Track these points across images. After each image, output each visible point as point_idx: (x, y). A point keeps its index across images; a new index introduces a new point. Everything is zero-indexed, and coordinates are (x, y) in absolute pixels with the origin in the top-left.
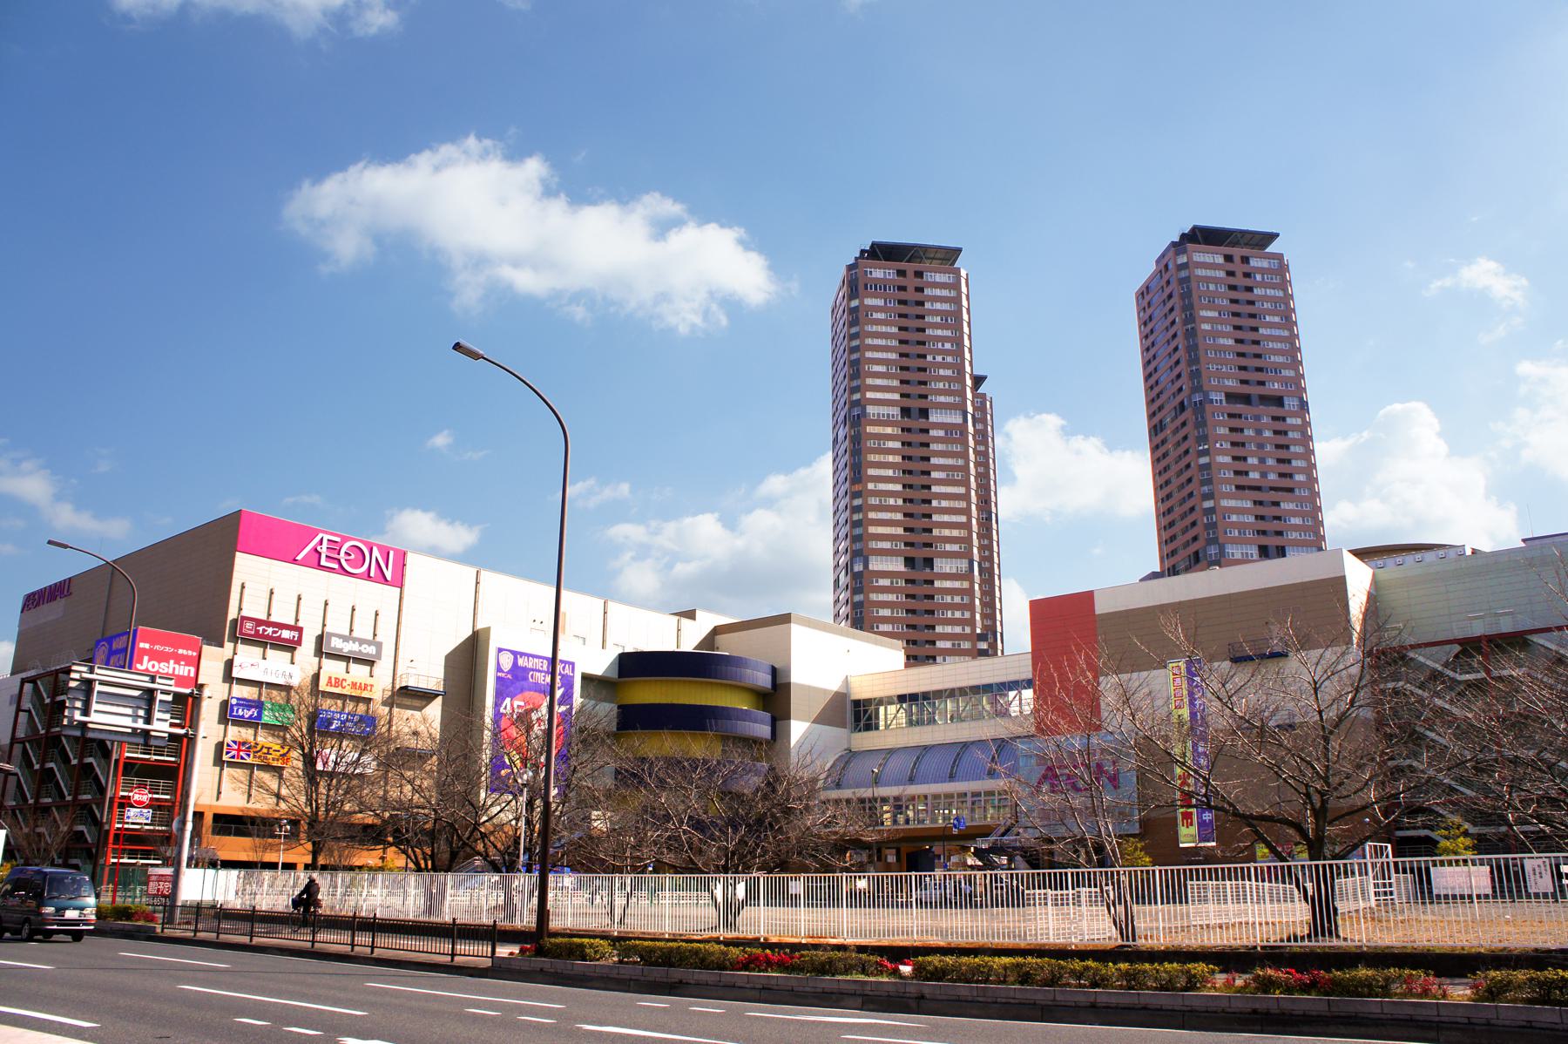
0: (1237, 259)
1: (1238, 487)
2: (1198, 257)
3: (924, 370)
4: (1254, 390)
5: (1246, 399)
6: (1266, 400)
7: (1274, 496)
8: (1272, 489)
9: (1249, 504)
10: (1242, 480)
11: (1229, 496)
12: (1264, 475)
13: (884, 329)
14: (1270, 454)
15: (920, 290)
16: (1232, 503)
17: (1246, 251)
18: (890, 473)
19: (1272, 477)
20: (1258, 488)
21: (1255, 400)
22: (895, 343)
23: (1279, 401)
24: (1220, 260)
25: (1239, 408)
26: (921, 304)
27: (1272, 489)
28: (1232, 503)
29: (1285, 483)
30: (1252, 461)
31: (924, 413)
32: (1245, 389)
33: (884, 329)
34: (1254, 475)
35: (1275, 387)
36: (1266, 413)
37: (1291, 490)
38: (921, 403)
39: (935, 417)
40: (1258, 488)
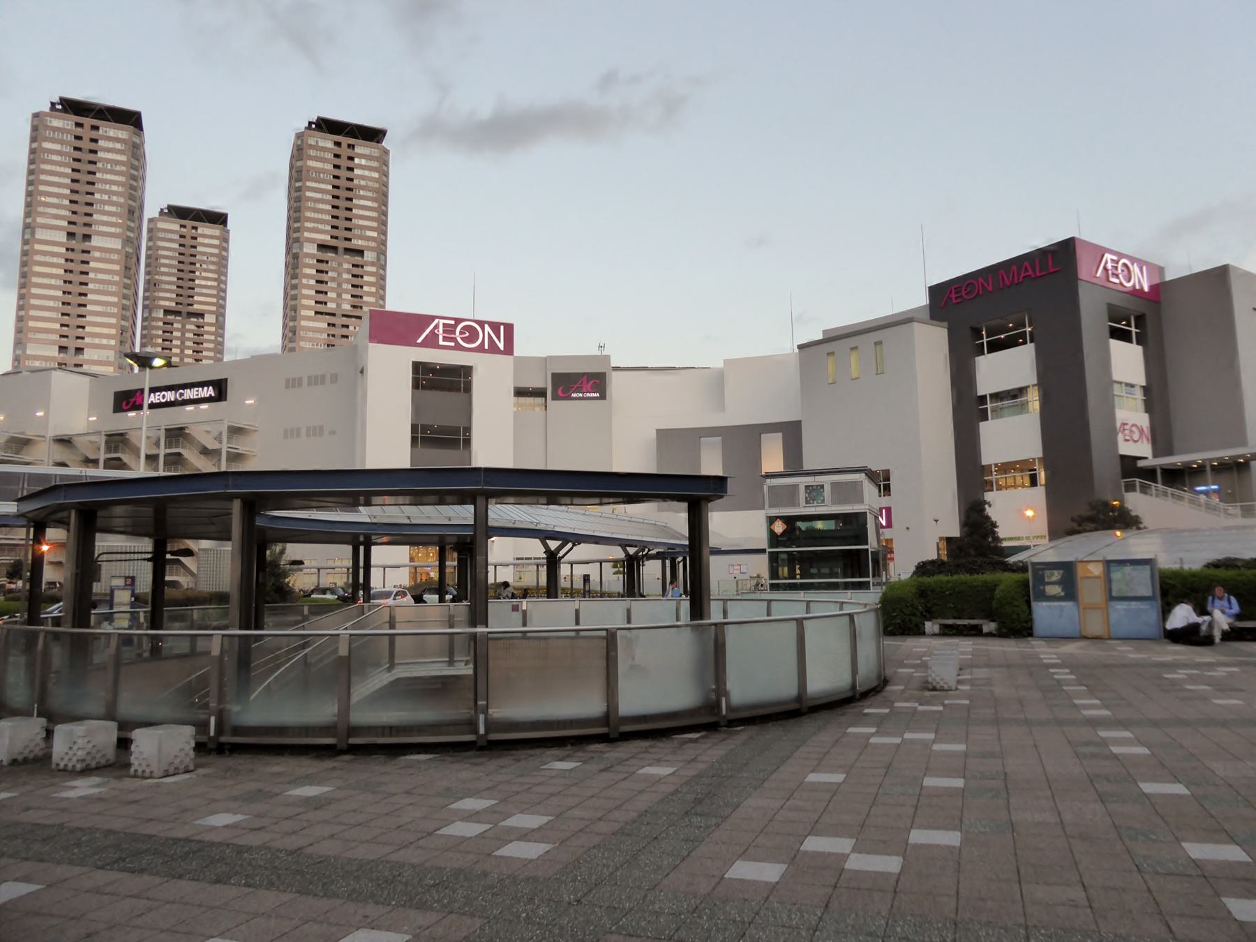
0: (344, 145)
1: (317, 313)
2: (312, 141)
3: (92, 205)
4: (342, 244)
5: (334, 249)
7: (345, 321)
8: (344, 316)
10: (321, 308)
11: (308, 318)
12: (339, 305)
13: (58, 169)
14: (346, 291)
15: (95, 141)
16: (311, 324)
17: (352, 141)
20: (334, 315)
21: (341, 251)
23: (360, 252)
24: (330, 145)
25: (329, 255)
26: (95, 152)
27: (344, 316)
28: (311, 324)
29: (357, 312)
30: (331, 295)
31: (87, 237)
32: (334, 243)
33: (58, 169)
34: (331, 306)
35: (357, 243)
36: (347, 263)
37: (360, 318)
38: (86, 231)
39: (96, 241)
40: (334, 315)
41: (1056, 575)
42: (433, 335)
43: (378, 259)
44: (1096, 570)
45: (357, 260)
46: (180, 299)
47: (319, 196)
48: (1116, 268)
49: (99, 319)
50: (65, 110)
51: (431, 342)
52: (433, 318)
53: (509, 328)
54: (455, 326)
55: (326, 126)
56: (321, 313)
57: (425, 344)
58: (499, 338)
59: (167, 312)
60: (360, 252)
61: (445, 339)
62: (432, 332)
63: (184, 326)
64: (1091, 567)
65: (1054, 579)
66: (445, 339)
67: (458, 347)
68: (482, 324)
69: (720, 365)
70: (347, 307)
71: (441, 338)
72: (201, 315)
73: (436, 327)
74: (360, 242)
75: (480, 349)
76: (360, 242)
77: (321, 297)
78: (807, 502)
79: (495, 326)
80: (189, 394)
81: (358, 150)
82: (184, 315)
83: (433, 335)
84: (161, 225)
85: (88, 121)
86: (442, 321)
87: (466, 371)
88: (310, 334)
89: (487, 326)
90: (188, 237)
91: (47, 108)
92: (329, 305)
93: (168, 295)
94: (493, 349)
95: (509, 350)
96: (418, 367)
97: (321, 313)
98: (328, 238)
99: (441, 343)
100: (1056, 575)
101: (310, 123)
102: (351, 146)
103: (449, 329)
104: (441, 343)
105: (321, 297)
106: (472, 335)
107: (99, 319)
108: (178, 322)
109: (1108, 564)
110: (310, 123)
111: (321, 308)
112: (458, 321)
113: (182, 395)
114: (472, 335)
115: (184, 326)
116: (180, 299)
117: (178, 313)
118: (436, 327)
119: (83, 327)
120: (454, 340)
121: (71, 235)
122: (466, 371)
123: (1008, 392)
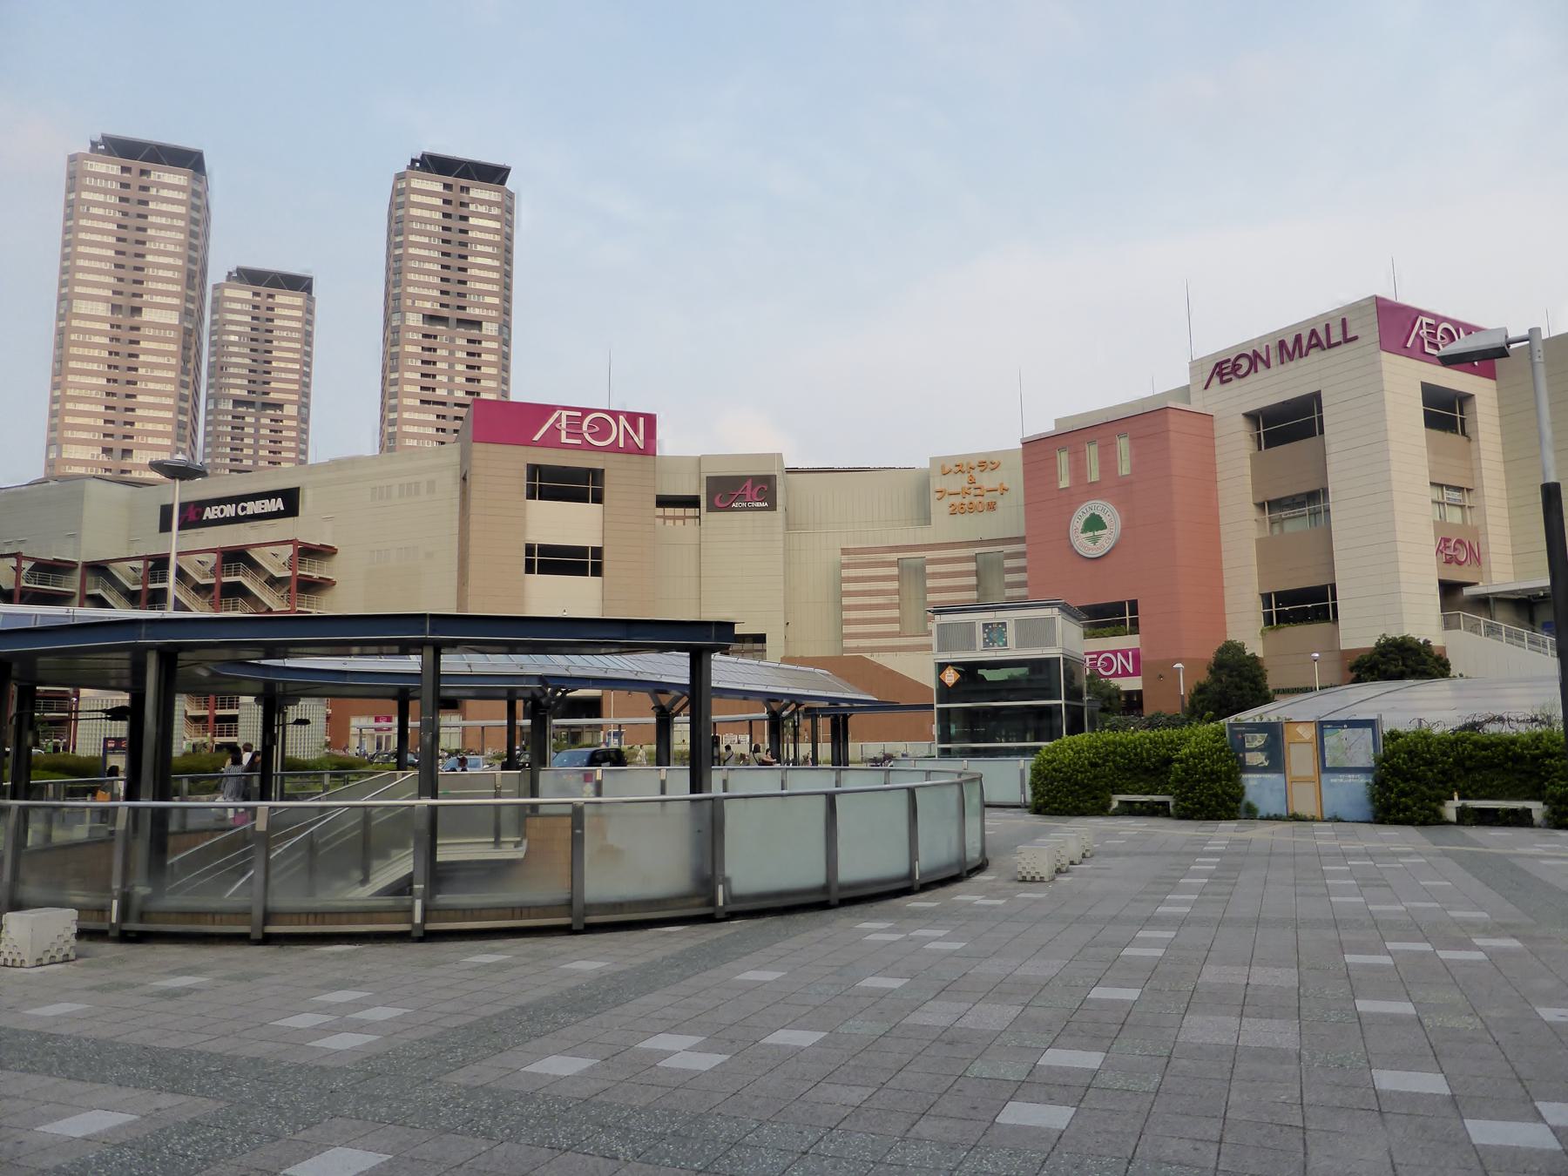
2: (416, 184)
6: (461, 322)
9: (433, 418)
10: (428, 395)
12: (451, 392)
16: (416, 416)
17: (464, 182)
18: (95, 367)
19: (460, 394)
20: (444, 404)
21: (453, 323)
22: (112, 240)
24: (439, 188)
28: (416, 416)
31: (137, 311)
32: (445, 312)
34: (441, 392)
35: (473, 312)
39: (148, 315)
40: (444, 404)
41: (1259, 740)
42: (554, 430)
43: (500, 331)
44: (1308, 733)
45: (474, 333)
46: (253, 387)
47: (425, 253)
48: (1435, 336)
49: (152, 413)
50: (108, 152)
51: (551, 440)
52: (553, 409)
53: (650, 420)
54: (582, 419)
55: (433, 164)
56: (428, 402)
57: (542, 443)
58: (636, 431)
59: (238, 403)
60: (477, 324)
61: (569, 435)
62: (553, 426)
63: (258, 420)
64: (1300, 729)
65: (1257, 744)
66: (569, 435)
67: (589, 447)
68: (615, 414)
69: (927, 466)
70: (460, 394)
71: (564, 434)
72: (280, 406)
73: (558, 420)
74: (477, 311)
75: (614, 448)
76: (477, 311)
77: (428, 382)
78: (986, 645)
79: (632, 418)
80: (253, 507)
81: (474, 193)
82: (258, 405)
83: (554, 430)
84: (228, 293)
85: (136, 165)
86: (565, 413)
87: (597, 475)
88: (415, 429)
89: (621, 418)
90: (263, 308)
91: (86, 149)
92: (438, 391)
93: (239, 381)
94: (631, 449)
95: (649, 449)
96: (534, 471)
97: (428, 402)
98: (437, 306)
99: (564, 439)
100: (1259, 740)
101: (414, 161)
102: (465, 189)
103: (574, 426)
104: (564, 439)
105: (428, 382)
106: (602, 429)
107: (152, 413)
108: (251, 415)
109: (1321, 726)
110: (414, 161)
111: (428, 395)
112: (586, 412)
113: (244, 509)
114: (602, 429)
115: (258, 420)
116: (253, 387)
117: (250, 404)
118: (558, 420)
119: (132, 424)
120: (580, 435)
121: (116, 308)
122: (597, 475)
123: (1293, 498)
